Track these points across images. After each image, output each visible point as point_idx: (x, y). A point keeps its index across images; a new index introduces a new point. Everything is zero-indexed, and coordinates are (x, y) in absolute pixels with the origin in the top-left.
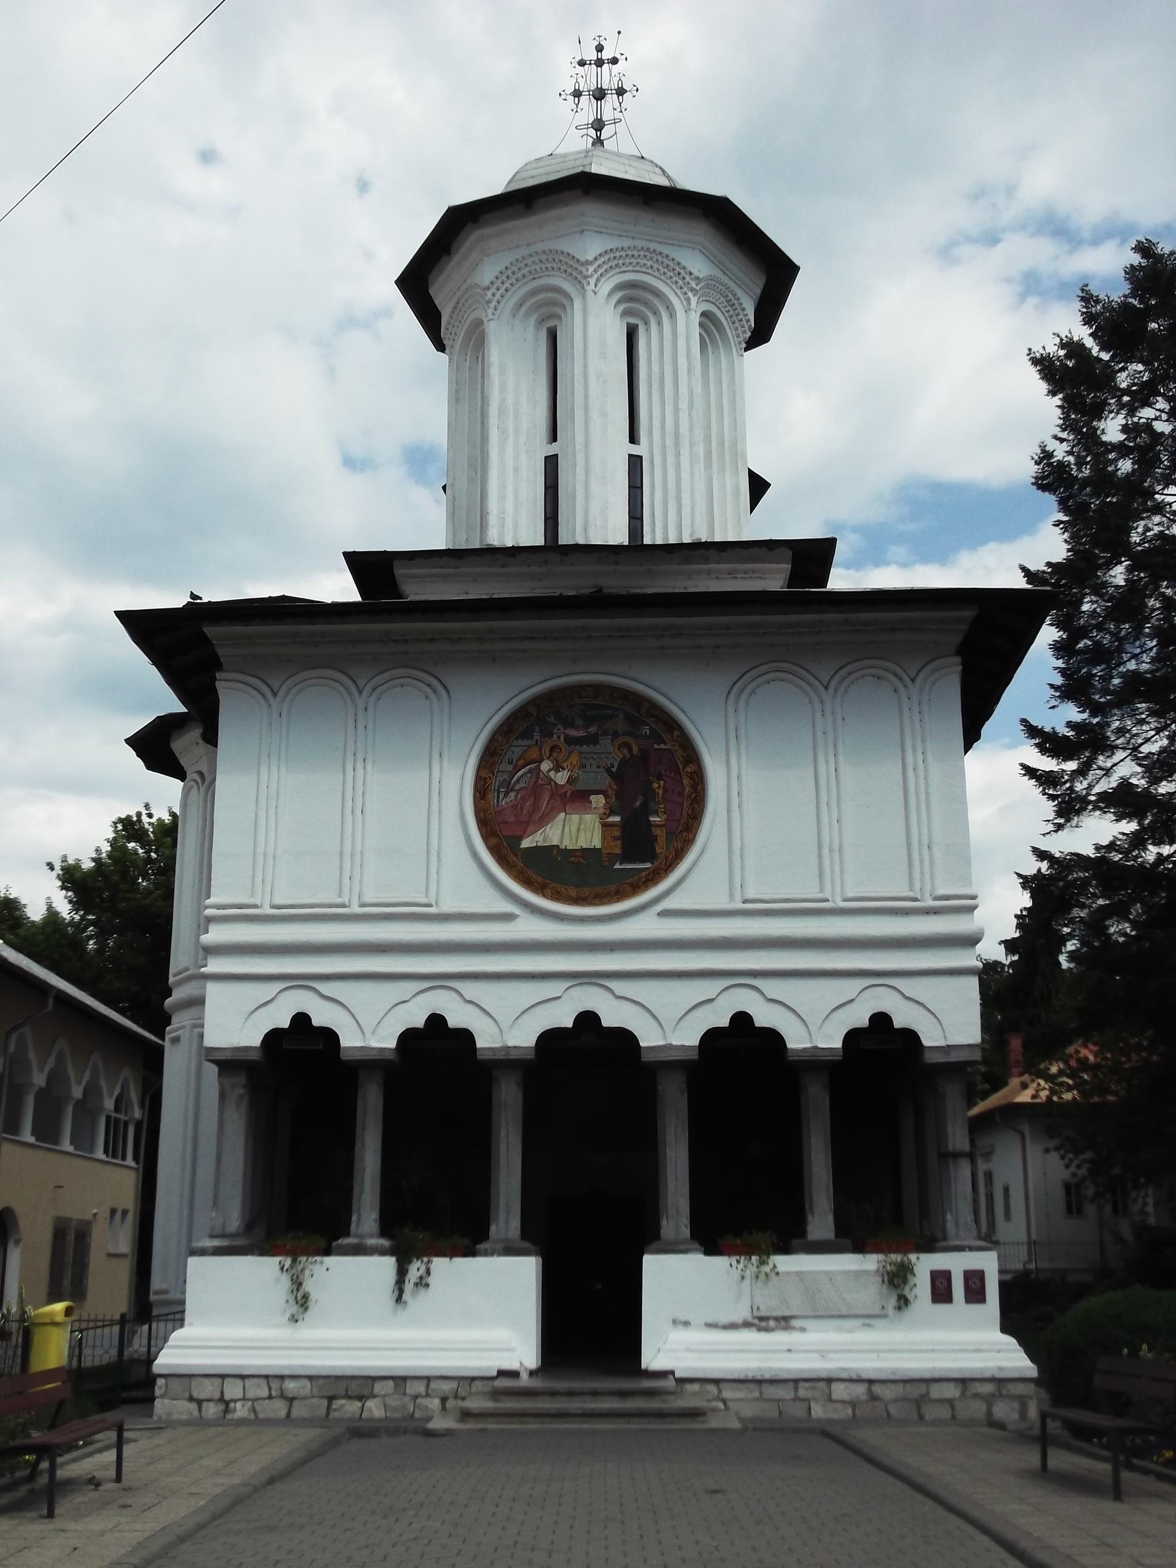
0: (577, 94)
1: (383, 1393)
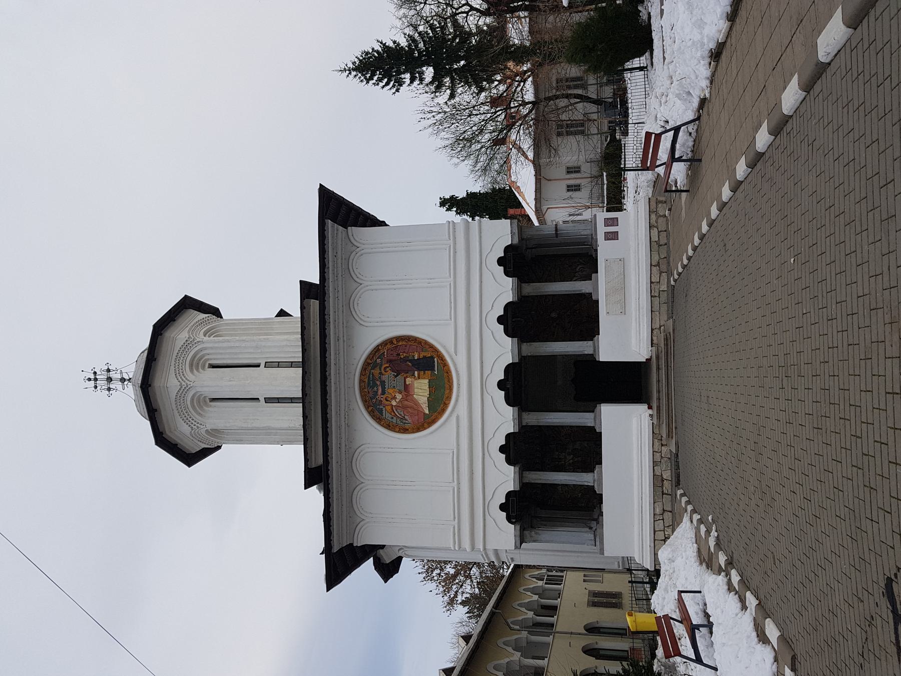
0: (109, 389)
1: (660, 471)
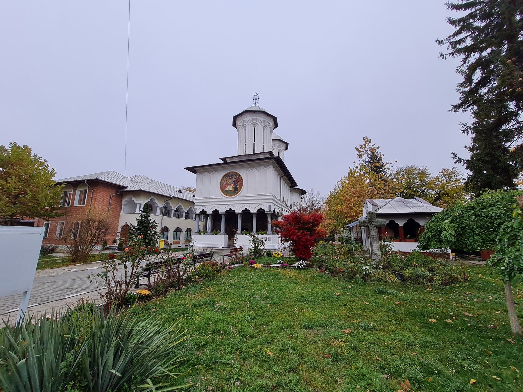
0: (253, 100)
